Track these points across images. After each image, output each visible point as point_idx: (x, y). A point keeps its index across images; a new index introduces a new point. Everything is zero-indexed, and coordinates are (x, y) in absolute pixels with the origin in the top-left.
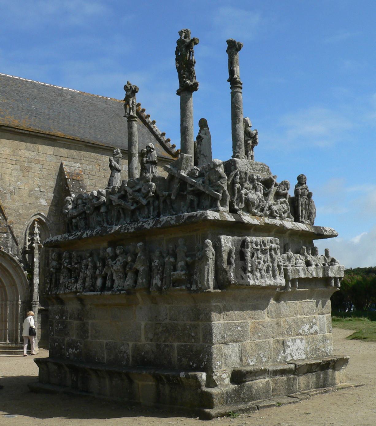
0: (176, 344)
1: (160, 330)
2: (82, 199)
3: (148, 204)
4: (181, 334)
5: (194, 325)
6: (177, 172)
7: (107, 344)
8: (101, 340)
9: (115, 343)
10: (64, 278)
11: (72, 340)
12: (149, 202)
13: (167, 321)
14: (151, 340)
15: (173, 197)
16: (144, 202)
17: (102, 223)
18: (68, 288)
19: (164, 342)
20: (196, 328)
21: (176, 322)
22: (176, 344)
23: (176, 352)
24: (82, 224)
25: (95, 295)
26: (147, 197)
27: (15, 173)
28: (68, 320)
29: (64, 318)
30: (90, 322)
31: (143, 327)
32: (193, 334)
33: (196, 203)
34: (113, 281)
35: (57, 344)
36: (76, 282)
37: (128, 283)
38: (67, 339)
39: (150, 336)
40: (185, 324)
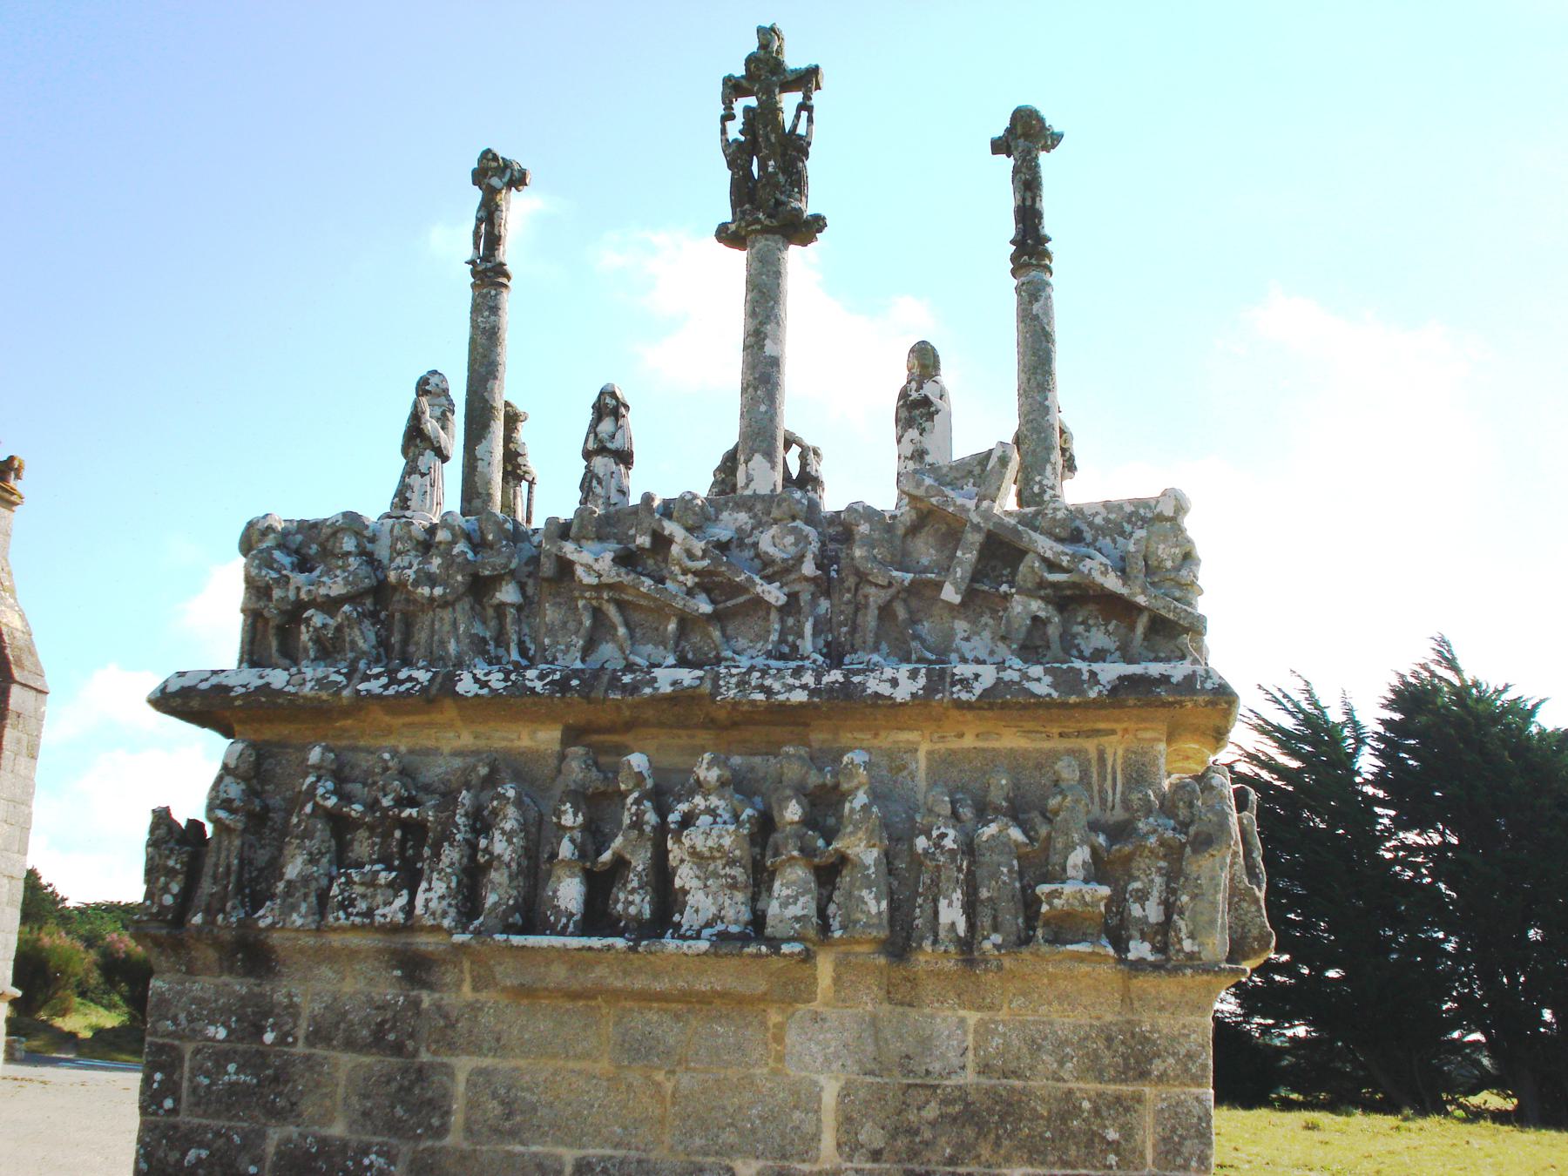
1: (931, 1111)
2: (358, 534)
3: (791, 606)
4: (1048, 1134)
5: (1118, 1099)
6: (977, 507)
8: (534, 1149)
9: (639, 1162)
10: (312, 860)
11: (323, 1142)
12: (793, 597)
13: (969, 1077)
14: (876, 1155)
15: (950, 594)
16: (774, 594)
17: (491, 647)
18: (342, 906)
19: (952, 1161)
20: (1127, 1110)
21: (1018, 1083)
24: (364, 638)
25: (590, 948)
26: (793, 576)
29: (269, 1037)
30: (464, 1065)
31: (829, 1098)
32: (1112, 1135)
33: (1053, 631)
35: (204, 1153)
36: (410, 879)
37: (795, 910)
38: (275, 1136)
39: (870, 1135)
40: (1070, 1092)
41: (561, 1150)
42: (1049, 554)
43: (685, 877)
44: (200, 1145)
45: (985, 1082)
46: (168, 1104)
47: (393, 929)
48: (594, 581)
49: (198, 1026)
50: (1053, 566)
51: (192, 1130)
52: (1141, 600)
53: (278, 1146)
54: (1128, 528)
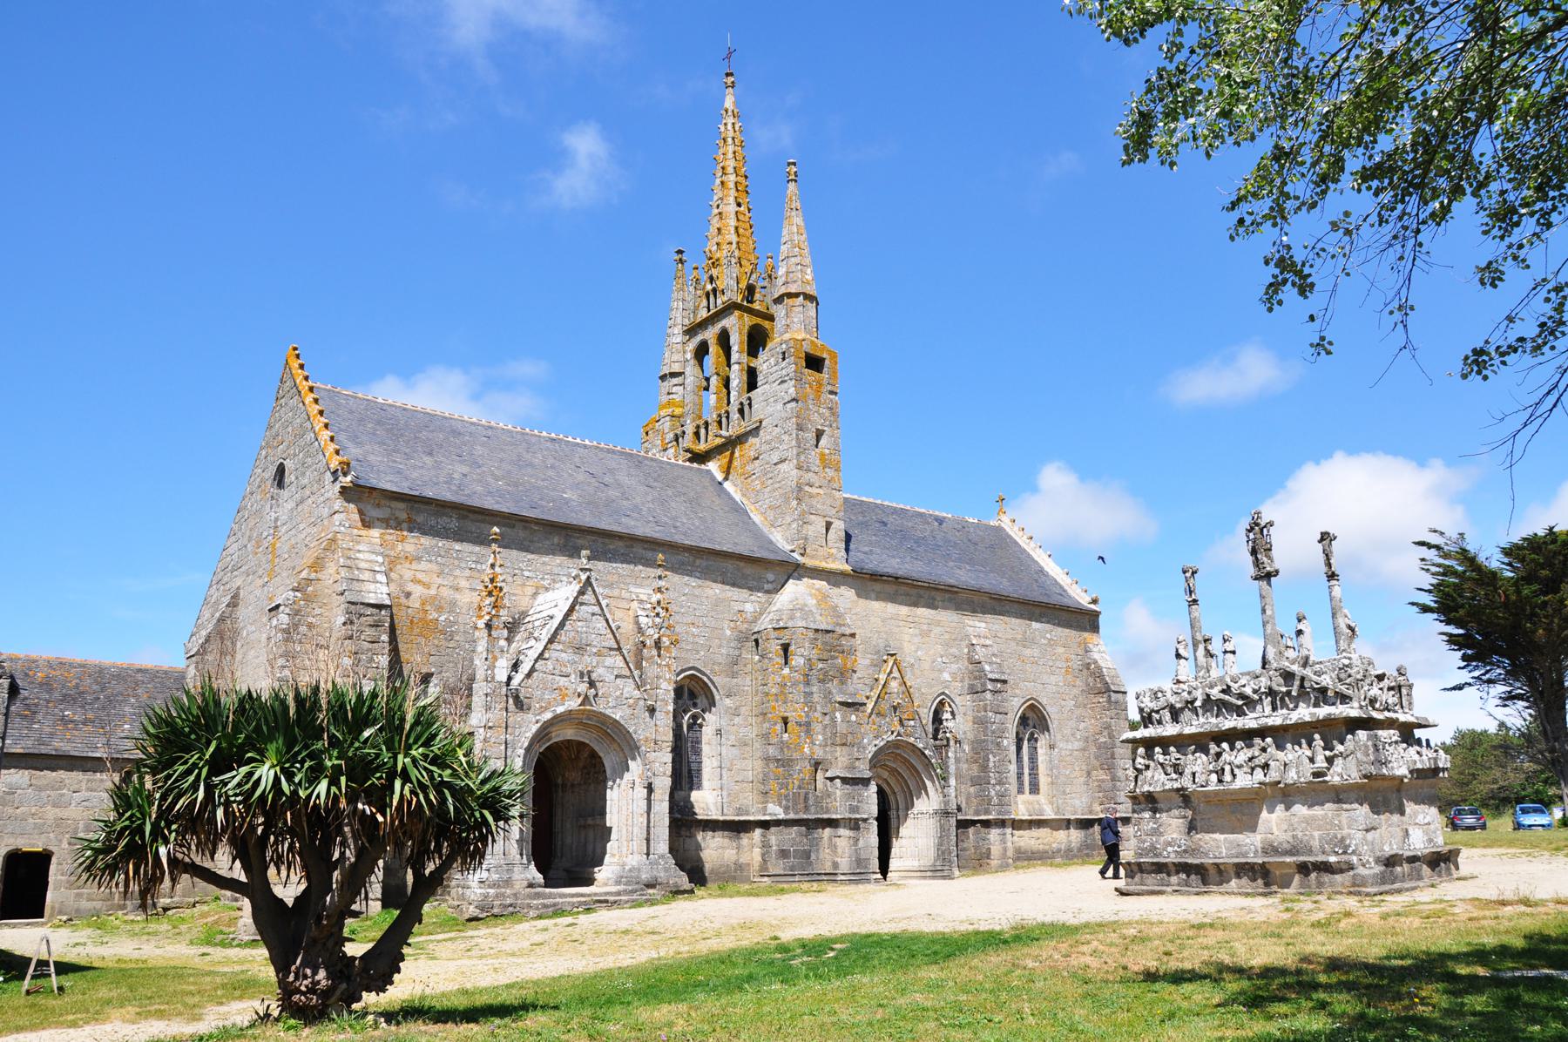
0: (1316, 834)
16: (1256, 697)
27: (916, 640)
34: (1234, 776)
43: (1236, 771)
47: (1178, 790)
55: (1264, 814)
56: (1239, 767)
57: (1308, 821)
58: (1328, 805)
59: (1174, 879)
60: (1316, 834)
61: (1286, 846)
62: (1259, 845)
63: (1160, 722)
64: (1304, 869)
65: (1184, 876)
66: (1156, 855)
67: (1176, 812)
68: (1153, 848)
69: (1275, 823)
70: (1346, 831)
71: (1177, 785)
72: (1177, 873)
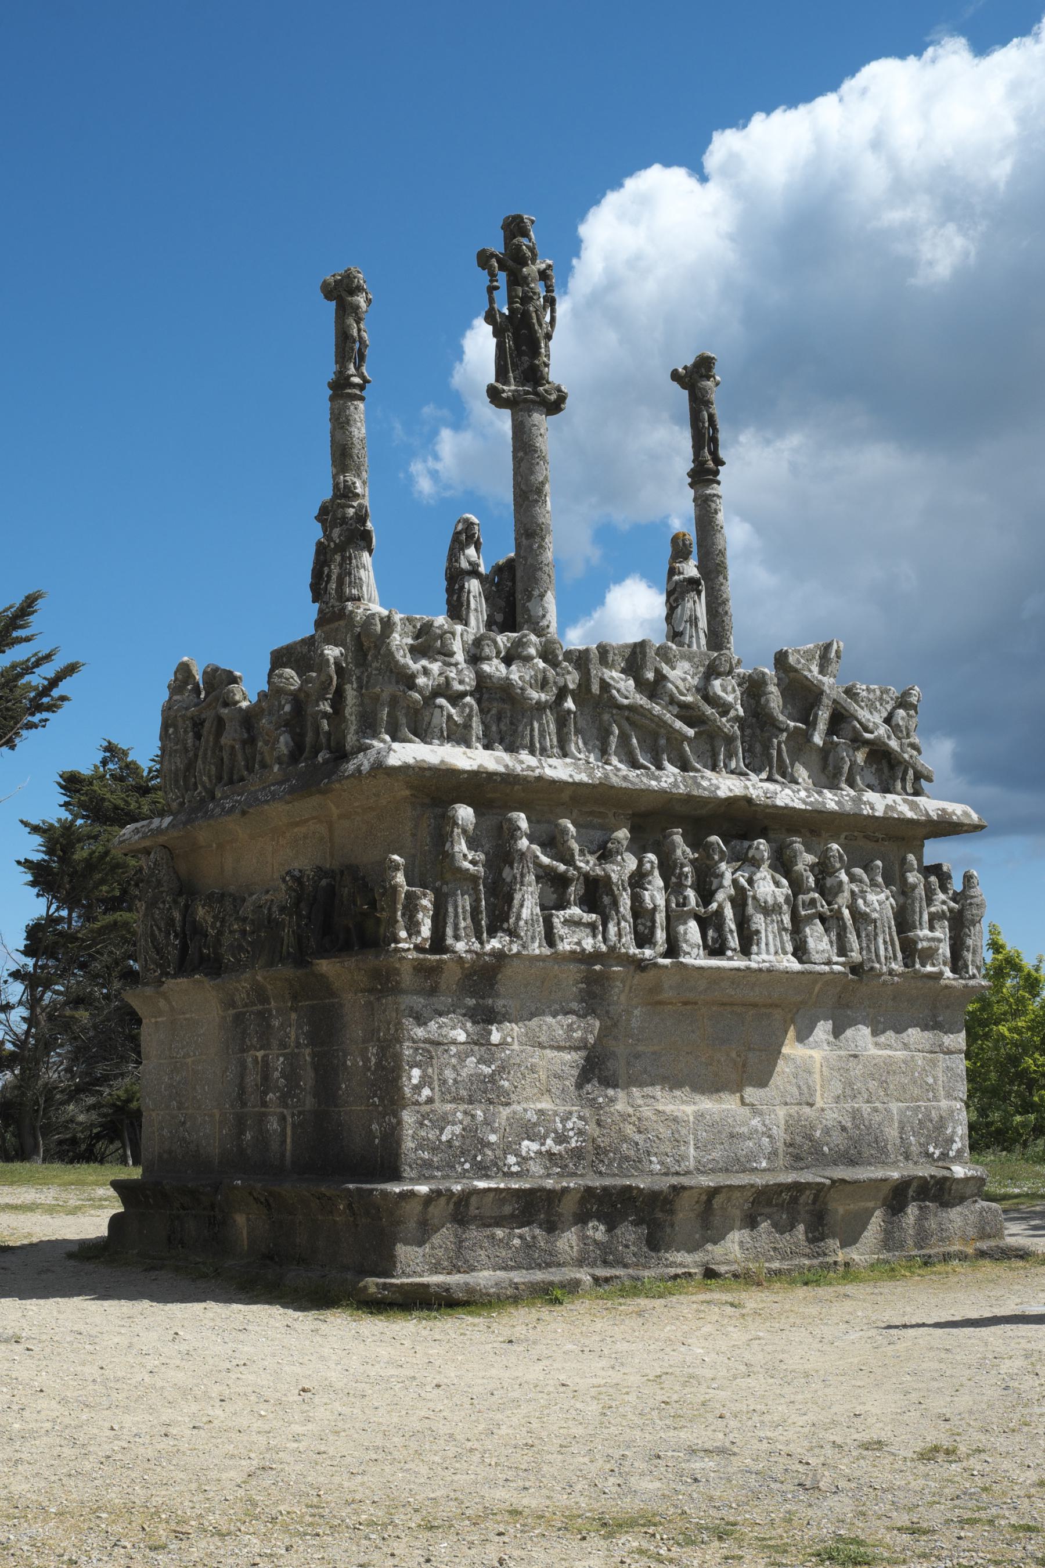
7: (700, 1116)
11: (541, 1112)
22: (894, 1107)
23: (896, 1125)
25: (738, 970)
28: (516, 1047)
38: (505, 1112)
41: (684, 1107)
42: (863, 720)
43: (759, 921)
44: (454, 1124)
45: (880, 1052)
46: (426, 1092)
47: (596, 956)
48: (626, 702)
49: (444, 1031)
50: (867, 730)
51: (446, 1113)
52: (906, 756)
53: (508, 1119)
54: (878, 704)
55: (791, 1048)
56: (767, 911)
57: (883, 1072)
58: (914, 1034)
59: (568, 1241)
60: (894, 1107)
61: (838, 1139)
62: (780, 1133)
63: (459, 736)
64: (897, 1197)
65: (597, 1231)
66: (482, 1170)
67: (555, 1025)
68: (473, 1139)
69: (821, 1072)
70: (944, 1104)
71: (588, 944)
72: (582, 1219)
